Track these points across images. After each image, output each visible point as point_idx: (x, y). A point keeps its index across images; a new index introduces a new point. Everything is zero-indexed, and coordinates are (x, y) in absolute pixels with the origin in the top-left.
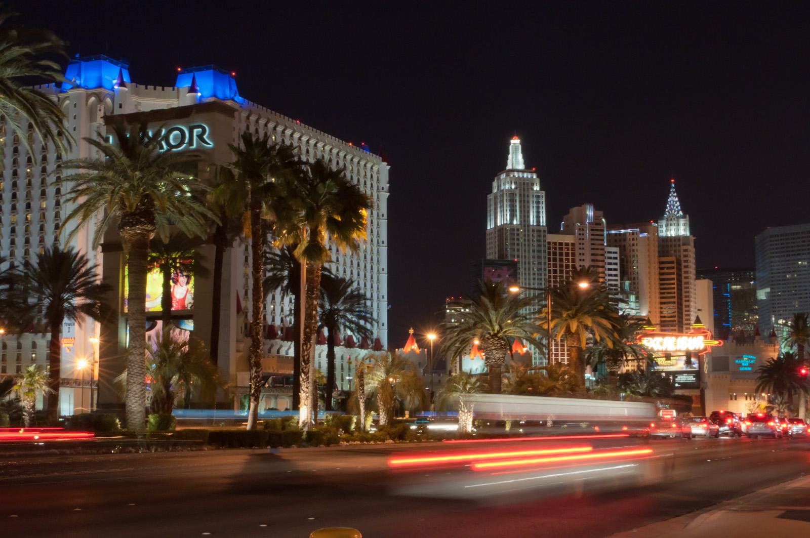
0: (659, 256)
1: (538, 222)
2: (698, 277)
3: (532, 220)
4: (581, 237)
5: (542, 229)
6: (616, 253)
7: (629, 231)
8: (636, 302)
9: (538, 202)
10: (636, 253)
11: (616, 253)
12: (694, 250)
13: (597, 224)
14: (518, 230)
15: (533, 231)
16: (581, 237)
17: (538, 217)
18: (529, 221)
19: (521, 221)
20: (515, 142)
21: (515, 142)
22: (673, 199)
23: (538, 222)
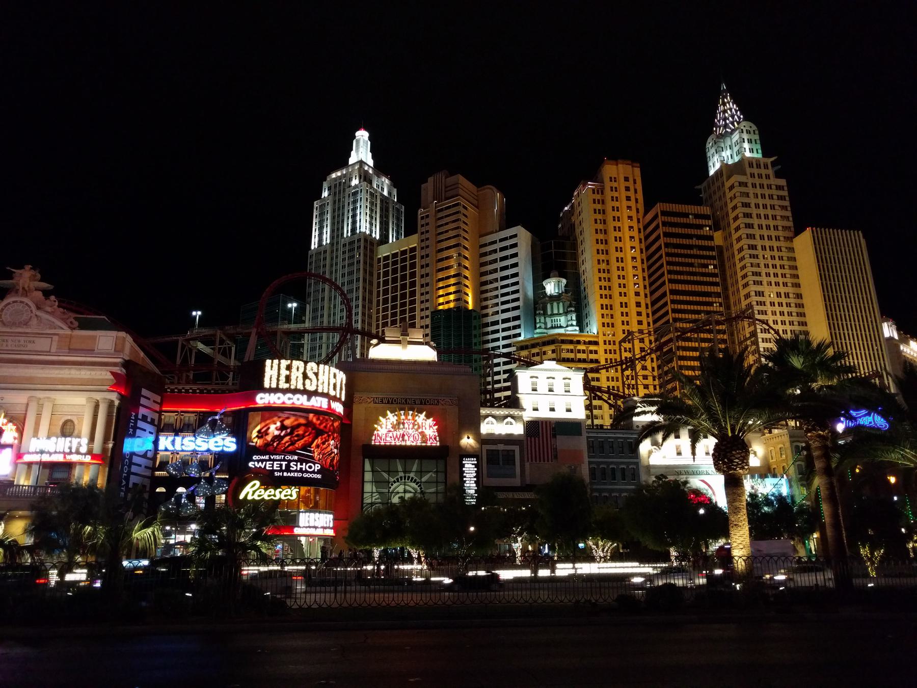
0: (646, 212)
1: (354, 230)
2: (798, 231)
3: (347, 231)
4: (423, 229)
5: (356, 237)
6: (515, 236)
7: (575, 193)
8: (566, 313)
9: (355, 202)
10: (584, 225)
11: (515, 236)
12: (783, 182)
13: (447, 199)
14: (325, 252)
15: (344, 245)
16: (423, 229)
17: (354, 222)
18: (343, 234)
19: (332, 238)
20: (362, 135)
21: (362, 135)
22: (728, 109)
23: (354, 230)
